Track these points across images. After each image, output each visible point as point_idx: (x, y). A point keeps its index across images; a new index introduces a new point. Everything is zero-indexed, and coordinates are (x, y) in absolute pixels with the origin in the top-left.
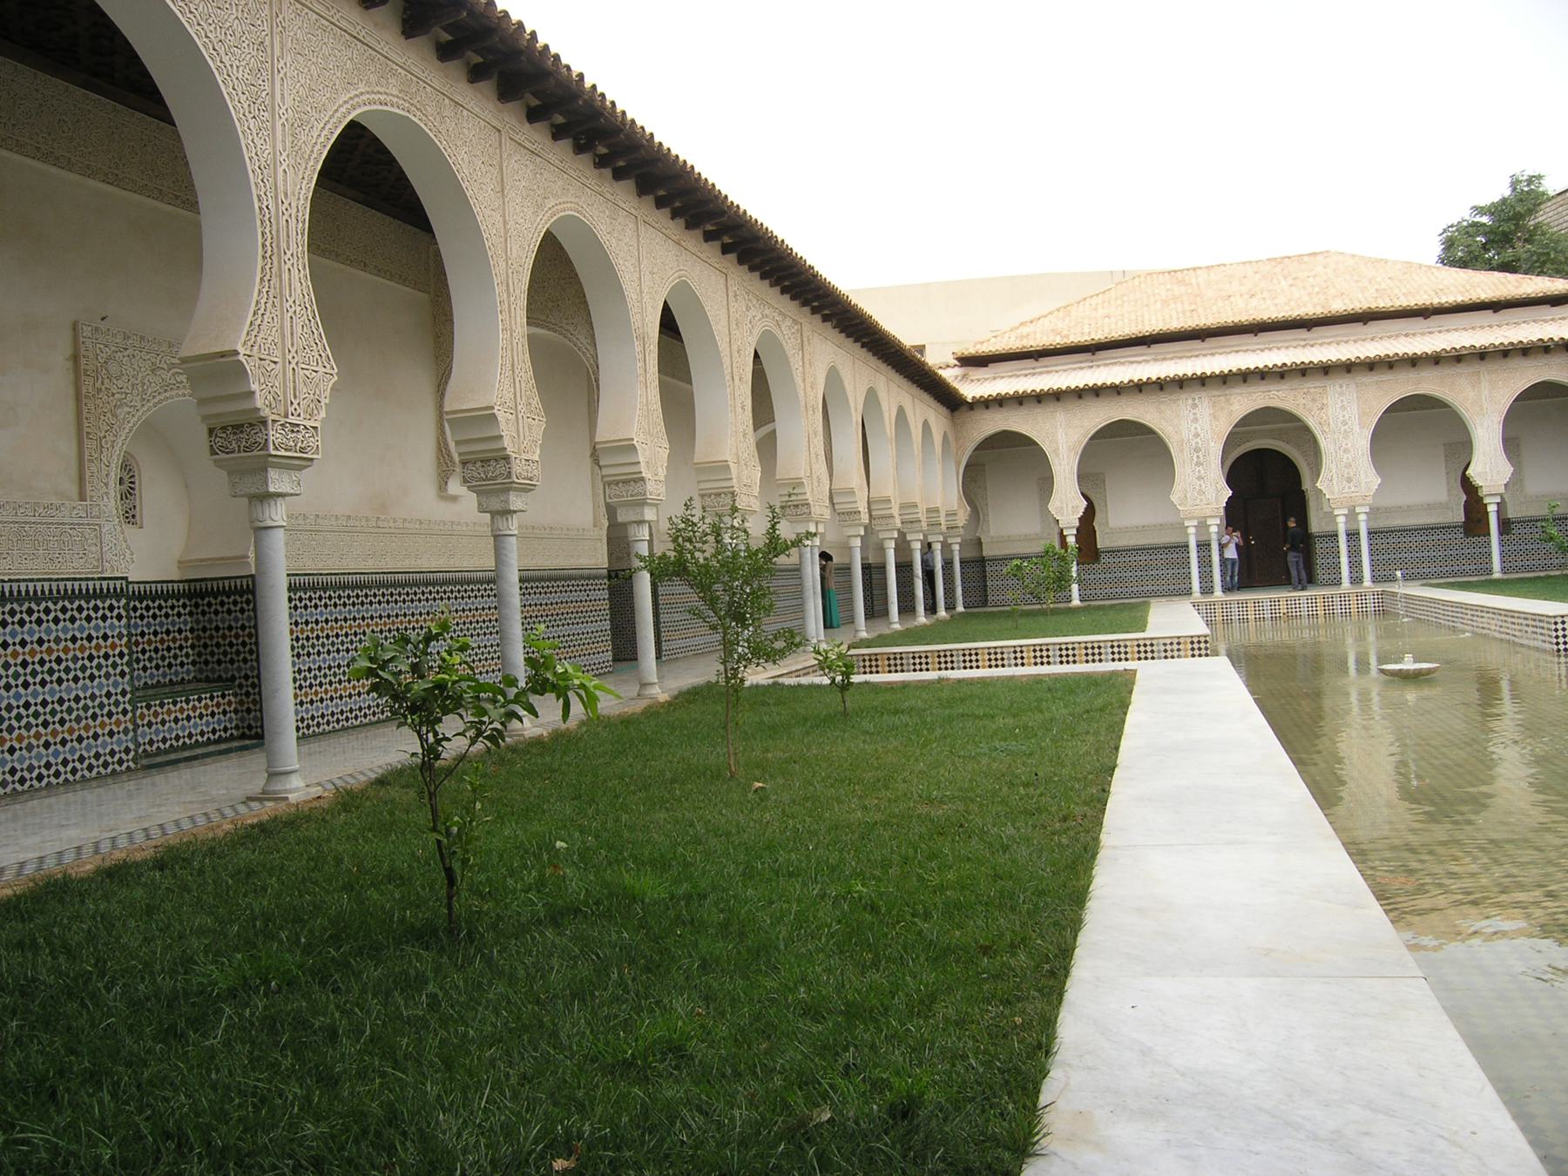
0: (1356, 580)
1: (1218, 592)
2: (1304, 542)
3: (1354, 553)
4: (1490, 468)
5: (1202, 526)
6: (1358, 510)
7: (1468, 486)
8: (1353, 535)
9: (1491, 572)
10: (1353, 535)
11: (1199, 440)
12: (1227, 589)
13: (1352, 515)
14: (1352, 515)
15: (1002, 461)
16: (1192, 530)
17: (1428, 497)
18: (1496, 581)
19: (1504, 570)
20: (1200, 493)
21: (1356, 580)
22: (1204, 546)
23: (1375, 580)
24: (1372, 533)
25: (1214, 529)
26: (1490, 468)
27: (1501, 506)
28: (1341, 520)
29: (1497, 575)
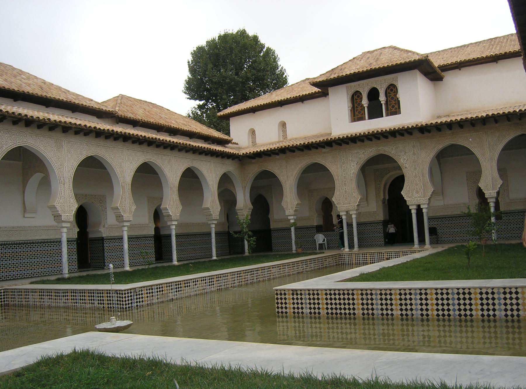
4: (490, 183)
7: (480, 193)
17: (459, 199)
26: (490, 183)
27: (497, 204)
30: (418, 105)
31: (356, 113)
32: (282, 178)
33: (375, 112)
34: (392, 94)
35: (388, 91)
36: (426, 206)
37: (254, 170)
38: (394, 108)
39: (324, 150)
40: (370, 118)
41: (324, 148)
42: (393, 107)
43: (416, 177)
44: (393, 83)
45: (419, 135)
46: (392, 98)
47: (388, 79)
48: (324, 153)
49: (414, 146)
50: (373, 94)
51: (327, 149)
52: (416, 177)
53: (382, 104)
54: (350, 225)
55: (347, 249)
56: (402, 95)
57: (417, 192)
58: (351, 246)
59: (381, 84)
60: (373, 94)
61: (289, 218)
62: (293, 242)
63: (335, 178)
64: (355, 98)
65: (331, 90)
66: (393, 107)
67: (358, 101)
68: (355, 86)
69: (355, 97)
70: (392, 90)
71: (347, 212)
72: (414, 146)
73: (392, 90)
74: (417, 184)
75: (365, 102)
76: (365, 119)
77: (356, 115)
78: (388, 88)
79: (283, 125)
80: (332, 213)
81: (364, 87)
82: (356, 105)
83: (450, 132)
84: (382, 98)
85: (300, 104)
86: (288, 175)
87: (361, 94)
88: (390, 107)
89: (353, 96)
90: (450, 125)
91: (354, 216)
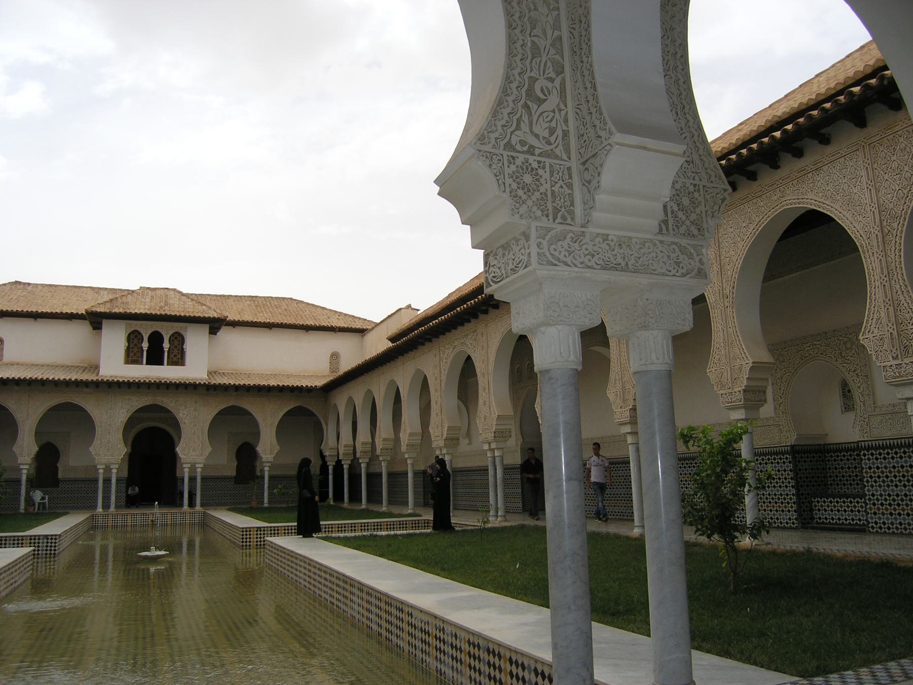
1: (112, 508)
2: (174, 481)
5: (108, 469)
6: (197, 466)
9: (263, 503)
10: (192, 479)
12: (117, 507)
13: (193, 468)
14: (193, 468)
16: (101, 471)
18: (266, 508)
19: (269, 502)
20: (107, 449)
21: (192, 504)
22: (107, 481)
23: (202, 505)
24: (203, 478)
25: (114, 471)
28: (186, 470)
29: (266, 505)
30: (200, 361)
31: (131, 354)
32: (18, 415)
33: (155, 358)
34: (176, 343)
36: (202, 466)
38: (178, 359)
40: (147, 363)
42: (175, 356)
43: (194, 434)
44: (182, 332)
46: (176, 347)
49: (196, 402)
50: (156, 339)
52: (194, 434)
53: (163, 352)
54: (107, 481)
55: (100, 510)
57: (194, 450)
58: (106, 506)
59: (167, 330)
60: (156, 339)
61: (22, 467)
63: (97, 424)
64: (134, 338)
65: (105, 323)
67: (136, 341)
70: (176, 338)
73: (178, 339)
75: (145, 345)
76: (142, 364)
77: (132, 357)
78: (173, 335)
84: (166, 345)
85: (32, 320)
87: (140, 333)
88: (172, 356)
90: (237, 388)
91: (114, 471)
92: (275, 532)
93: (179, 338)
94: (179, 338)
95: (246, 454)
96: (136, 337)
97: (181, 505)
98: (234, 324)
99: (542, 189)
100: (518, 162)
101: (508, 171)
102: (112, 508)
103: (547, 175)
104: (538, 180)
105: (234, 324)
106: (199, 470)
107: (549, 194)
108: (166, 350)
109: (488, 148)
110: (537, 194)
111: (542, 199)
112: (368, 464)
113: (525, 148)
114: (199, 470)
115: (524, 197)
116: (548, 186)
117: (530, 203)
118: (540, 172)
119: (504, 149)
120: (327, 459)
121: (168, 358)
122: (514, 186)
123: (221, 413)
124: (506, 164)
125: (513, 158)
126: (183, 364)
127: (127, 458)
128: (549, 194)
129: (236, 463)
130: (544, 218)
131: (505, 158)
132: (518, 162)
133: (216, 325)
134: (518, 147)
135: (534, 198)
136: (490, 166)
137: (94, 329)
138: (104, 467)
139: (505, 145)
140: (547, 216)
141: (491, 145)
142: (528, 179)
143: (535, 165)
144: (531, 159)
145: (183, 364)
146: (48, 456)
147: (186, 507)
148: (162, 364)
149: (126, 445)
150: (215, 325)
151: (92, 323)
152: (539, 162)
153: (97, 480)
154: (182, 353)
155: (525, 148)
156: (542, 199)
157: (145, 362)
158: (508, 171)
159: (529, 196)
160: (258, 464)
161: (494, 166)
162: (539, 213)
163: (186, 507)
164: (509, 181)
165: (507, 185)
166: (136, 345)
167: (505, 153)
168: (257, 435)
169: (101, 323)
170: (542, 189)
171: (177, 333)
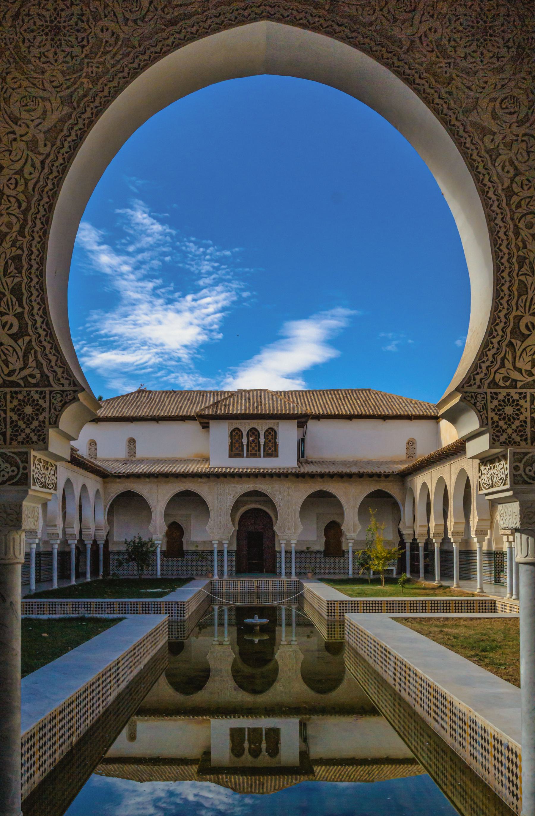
0: (288, 574)
1: (226, 576)
2: (274, 555)
3: (288, 561)
5: (221, 543)
8: (288, 552)
9: (347, 573)
11: (221, 501)
13: (288, 543)
15: (128, 503)
16: (215, 546)
21: (288, 574)
23: (297, 575)
24: (297, 552)
25: (226, 546)
31: (234, 449)
32: (150, 502)
34: (270, 437)
35: (267, 433)
36: (295, 542)
37: (118, 488)
38: (272, 451)
39: (200, 480)
40: (247, 456)
41: (201, 478)
42: (270, 449)
45: (294, 479)
46: (270, 441)
47: (270, 423)
48: (201, 482)
49: (289, 488)
51: (204, 480)
52: (288, 515)
54: (221, 553)
55: (216, 577)
56: (281, 440)
58: (221, 574)
59: (262, 427)
62: (159, 567)
63: (210, 507)
64: (235, 434)
65: (212, 423)
66: (270, 449)
68: (237, 424)
69: (234, 433)
70: (270, 433)
71: (219, 542)
72: (289, 488)
73: (272, 433)
74: (289, 522)
76: (243, 457)
77: (235, 451)
78: (267, 430)
79: (132, 441)
80: (183, 540)
81: (245, 426)
82: (234, 441)
83: (321, 480)
84: (262, 440)
86: (158, 498)
87: (240, 430)
88: (267, 448)
89: (231, 433)
92: (355, 607)
93: (273, 433)
94: (273, 433)
95: (333, 530)
96: (237, 433)
97: (280, 575)
98: (318, 417)
99: (522, 418)
100: (501, 397)
101: (490, 406)
102: (226, 576)
103: (527, 405)
104: (519, 410)
105: (318, 417)
106: (293, 545)
107: (529, 420)
108: (262, 444)
109: (474, 389)
110: (517, 423)
111: (521, 426)
112: (442, 544)
113: (508, 384)
114: (293, 545)
115: (505, 427)
116: (528, 414)
117: (510, 431)
118: (522, 402)
119: (489, 387)
120: (405, 537)
121: (264, 451)
122: (496, 418)
123: (310, 496)
124: (489, 398)
125: (496, 394)
126: (277, 456)
127: (235, 534)
128: (529, 420)
129: (324, 539)
130: (523, 443)
131: (489, 395)
132: (501, 397)
133: (303, 420)
134: (501, 383)
135: (514, 427)
136: (475, 404)
137: (204, 427)
138: (217, 542)
139: (489, 384)
140: (526, 440)
141: (476, 386)
142: (509, 410)
143: (516, 397)
144: (513, 392)
145: (277, 456)
146: (175, 531)
147: (283, 577)
148: (260, 456)
149: (234, 525)
150: (302, 420)
151: (201, 423)
152: (520, 394)
153: (212, 552)
154: (276, 445)
155: (508, 384)
156: (521, 426)
157: (245, 455)
158: (490, 406)
159: (509, 425)
160: (343, 540)
161: (478, 404)
162: (518, 439)
163: (283, 577)
164: (491, 414)
165: (489, 419)
166: (237, 441)
167: (488, 391)
168: (342, 514)
169: (208, 423)
170: (522, 418)
171: (270, 428)
